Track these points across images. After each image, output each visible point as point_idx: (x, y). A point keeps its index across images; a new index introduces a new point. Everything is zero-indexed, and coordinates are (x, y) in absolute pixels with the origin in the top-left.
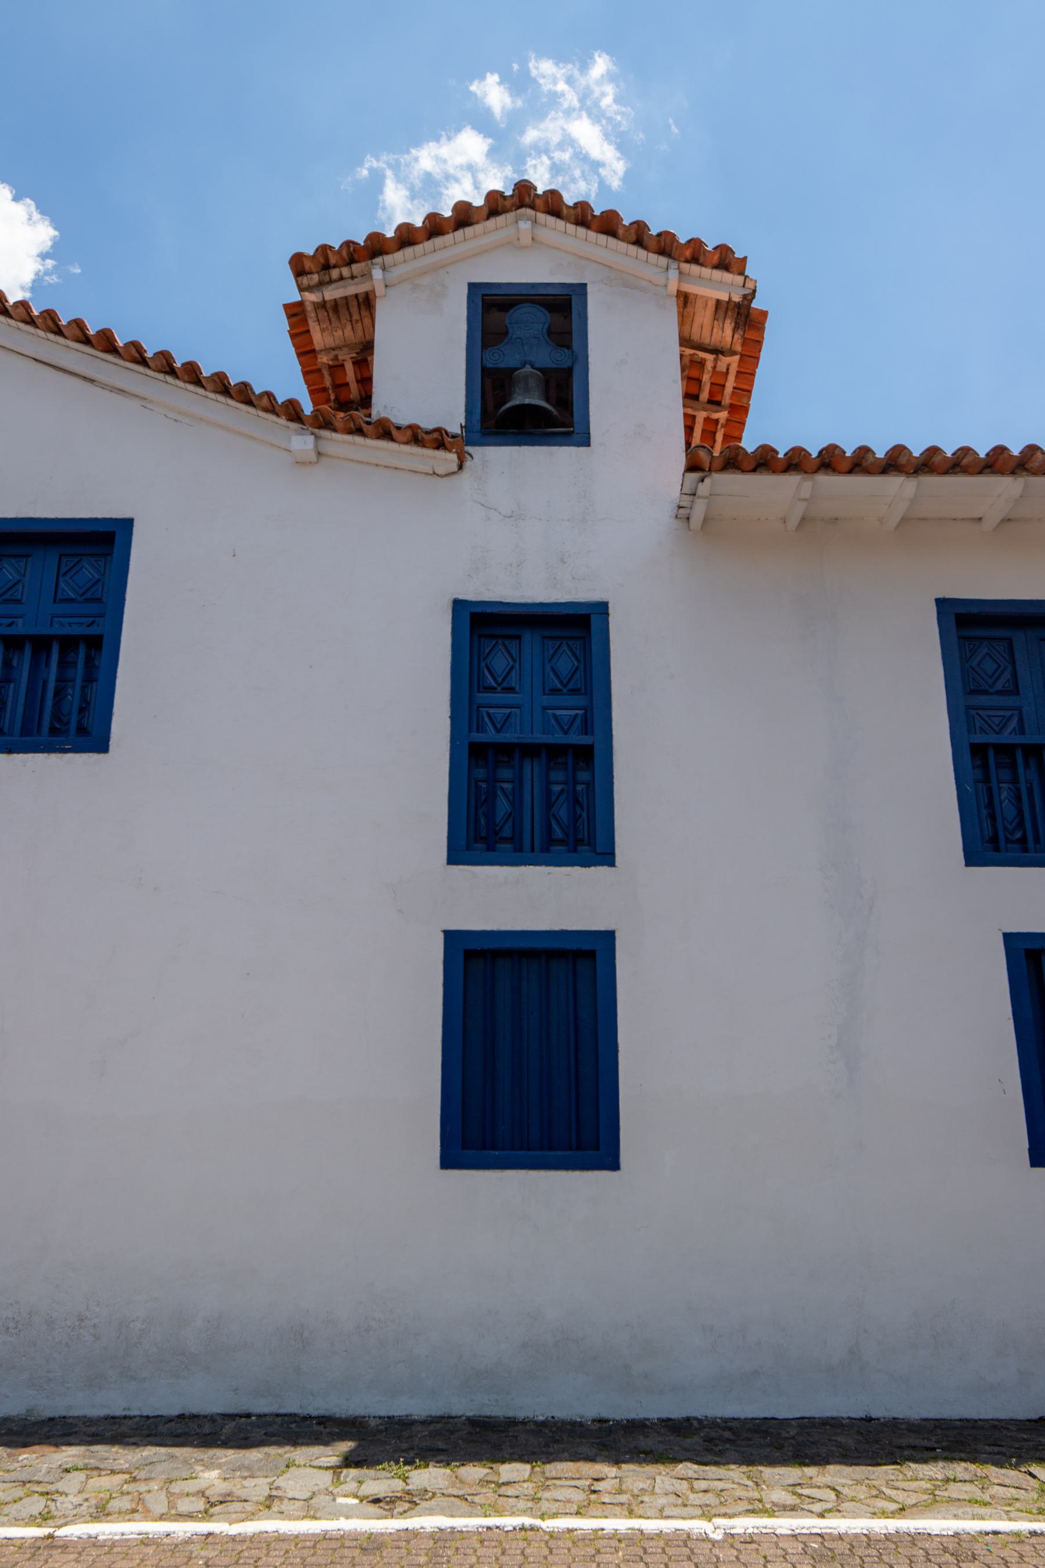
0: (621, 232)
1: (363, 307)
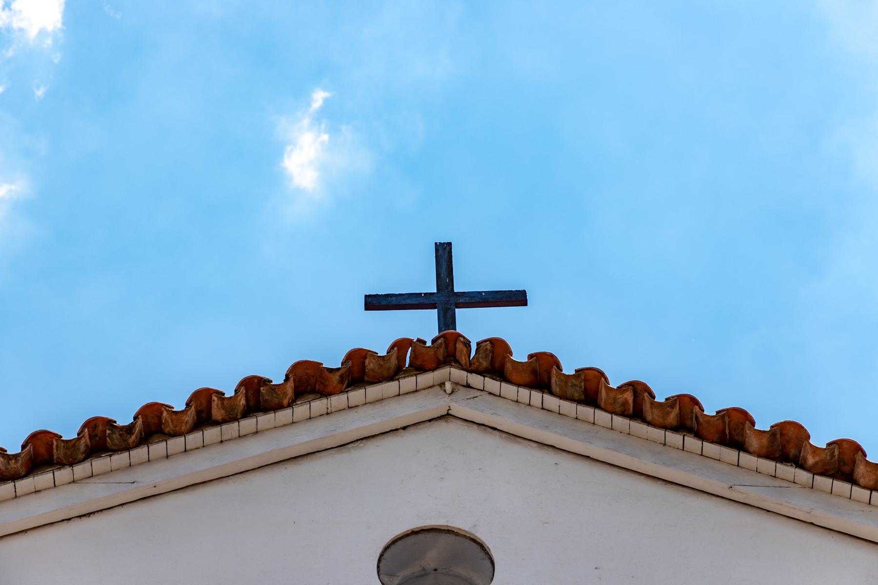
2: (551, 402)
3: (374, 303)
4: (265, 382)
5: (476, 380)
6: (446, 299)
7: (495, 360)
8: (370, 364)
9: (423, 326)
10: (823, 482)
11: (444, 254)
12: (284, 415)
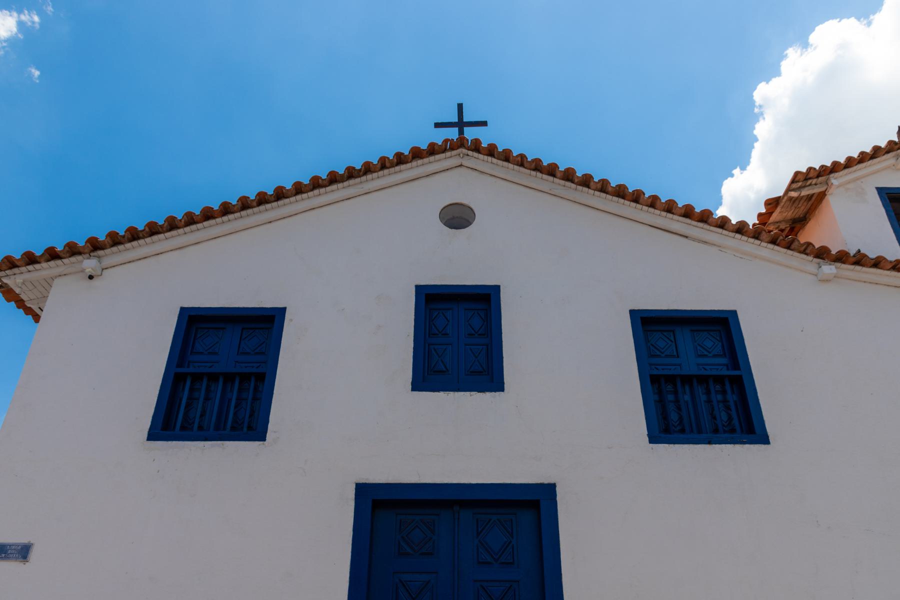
2: (495, 160)
3: (438, 125)
4: (402, 154)
5: (470, 153)
6: (461, 124)
7: (476, 147)
8: (436, 148)
9: (452, 134)
10: (580, 188)
11: (460, 107)
12: (409, 165)
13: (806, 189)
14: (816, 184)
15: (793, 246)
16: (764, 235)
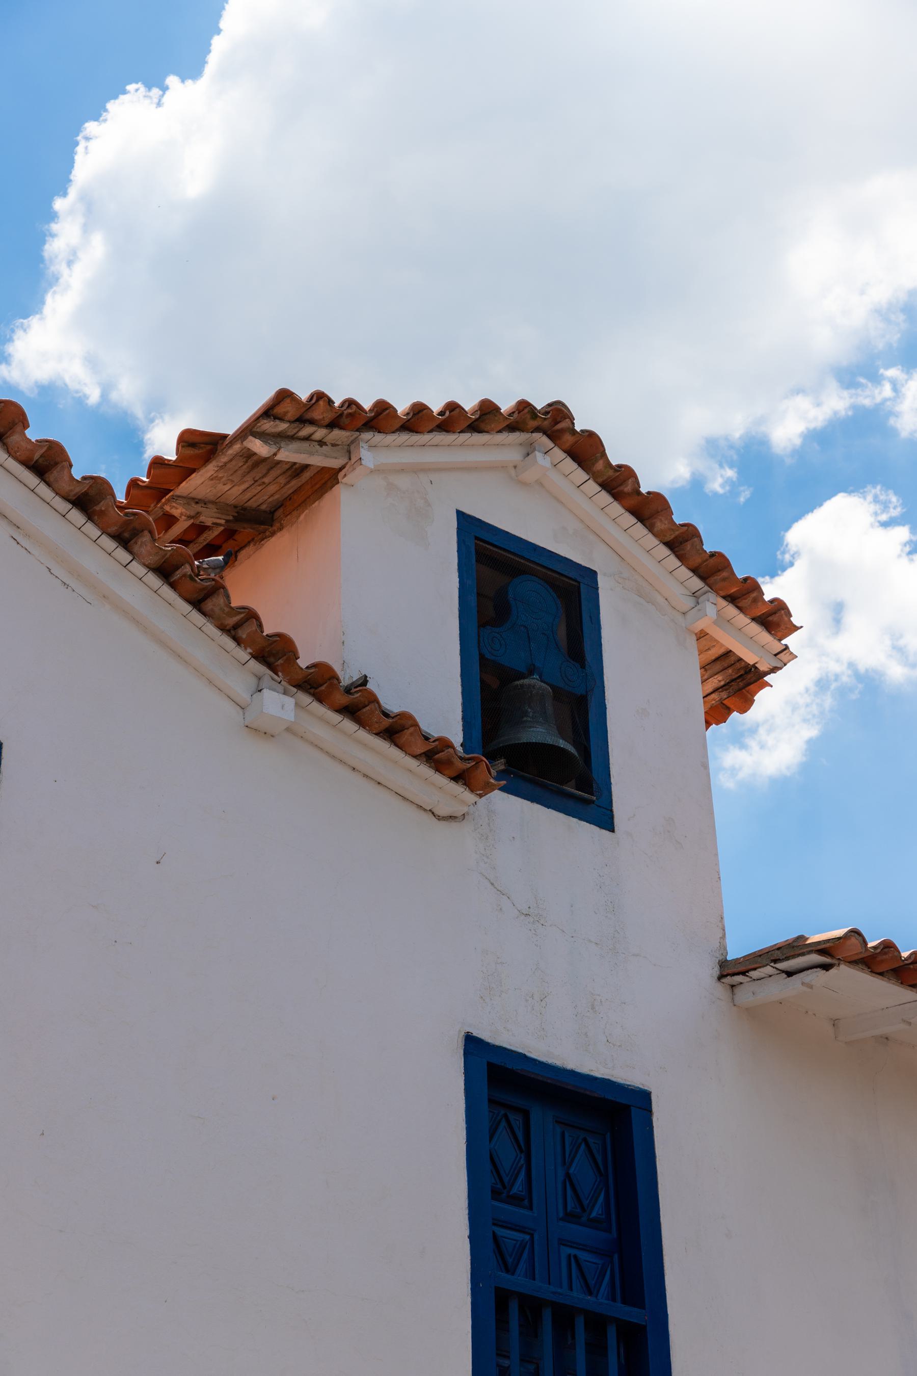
0: (660, 525)
1: (290, 473)
13: (295, 445)
14: (321, 443)
15: (209, 605)
16: (144, 544)
